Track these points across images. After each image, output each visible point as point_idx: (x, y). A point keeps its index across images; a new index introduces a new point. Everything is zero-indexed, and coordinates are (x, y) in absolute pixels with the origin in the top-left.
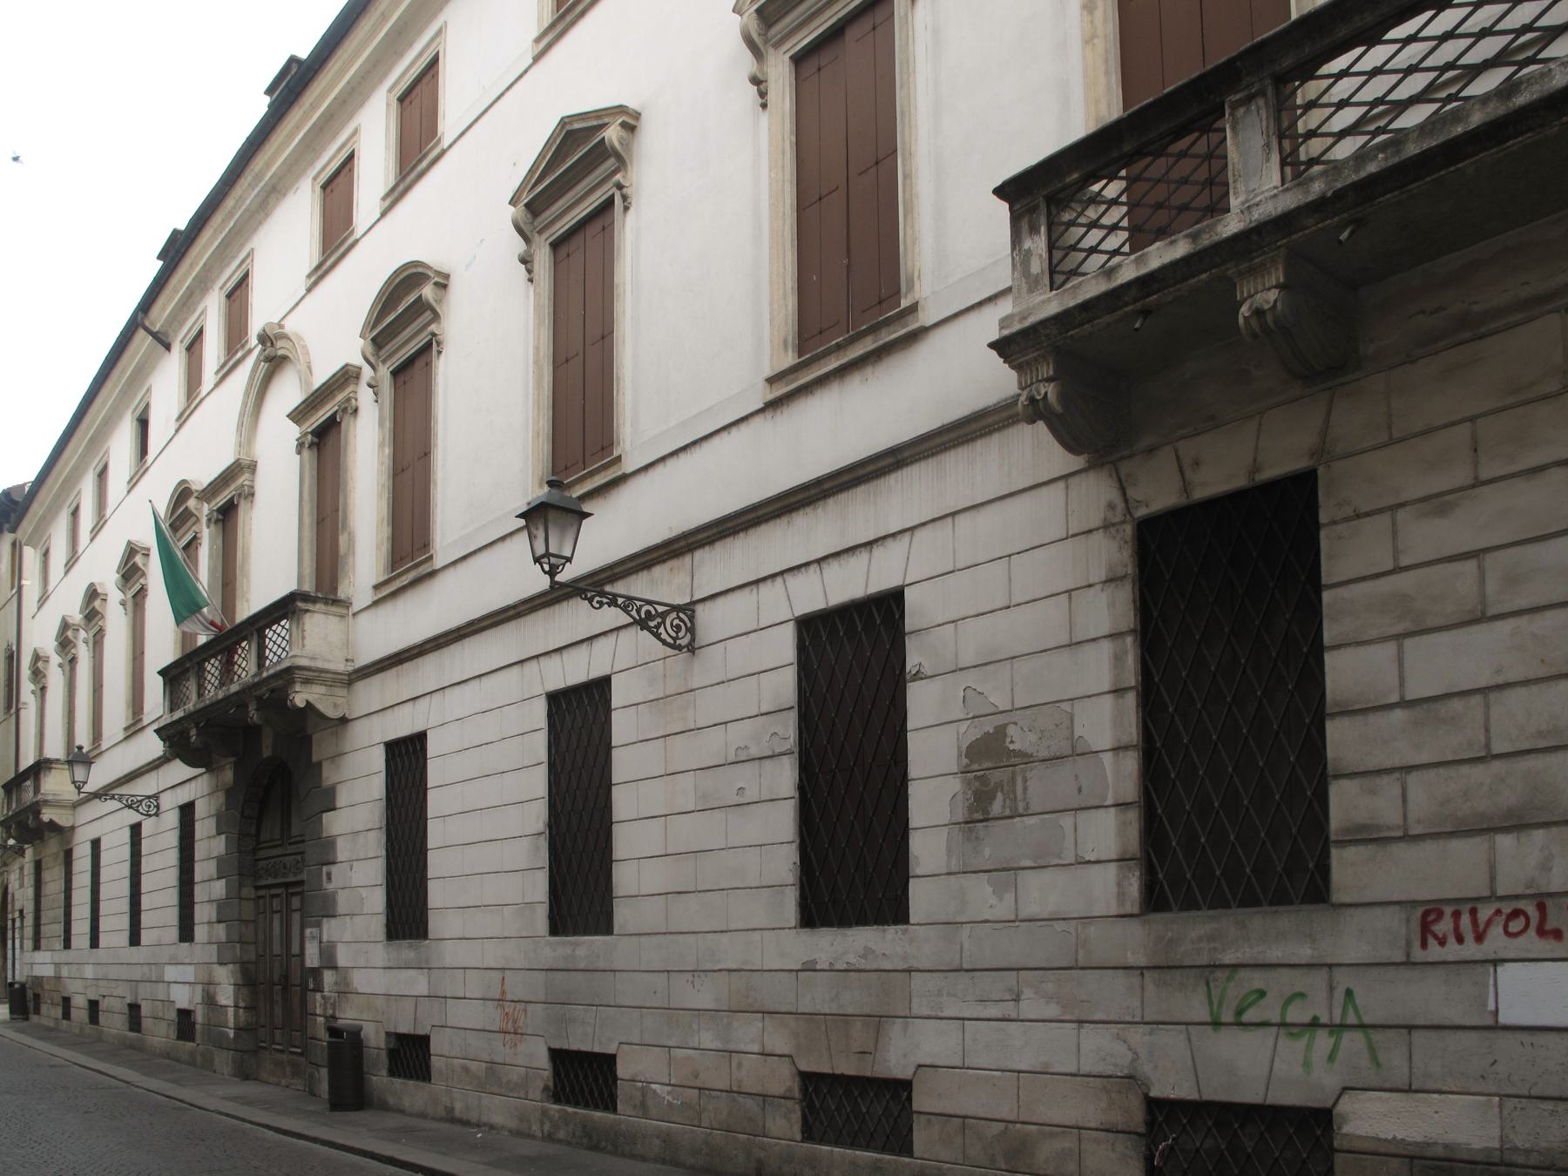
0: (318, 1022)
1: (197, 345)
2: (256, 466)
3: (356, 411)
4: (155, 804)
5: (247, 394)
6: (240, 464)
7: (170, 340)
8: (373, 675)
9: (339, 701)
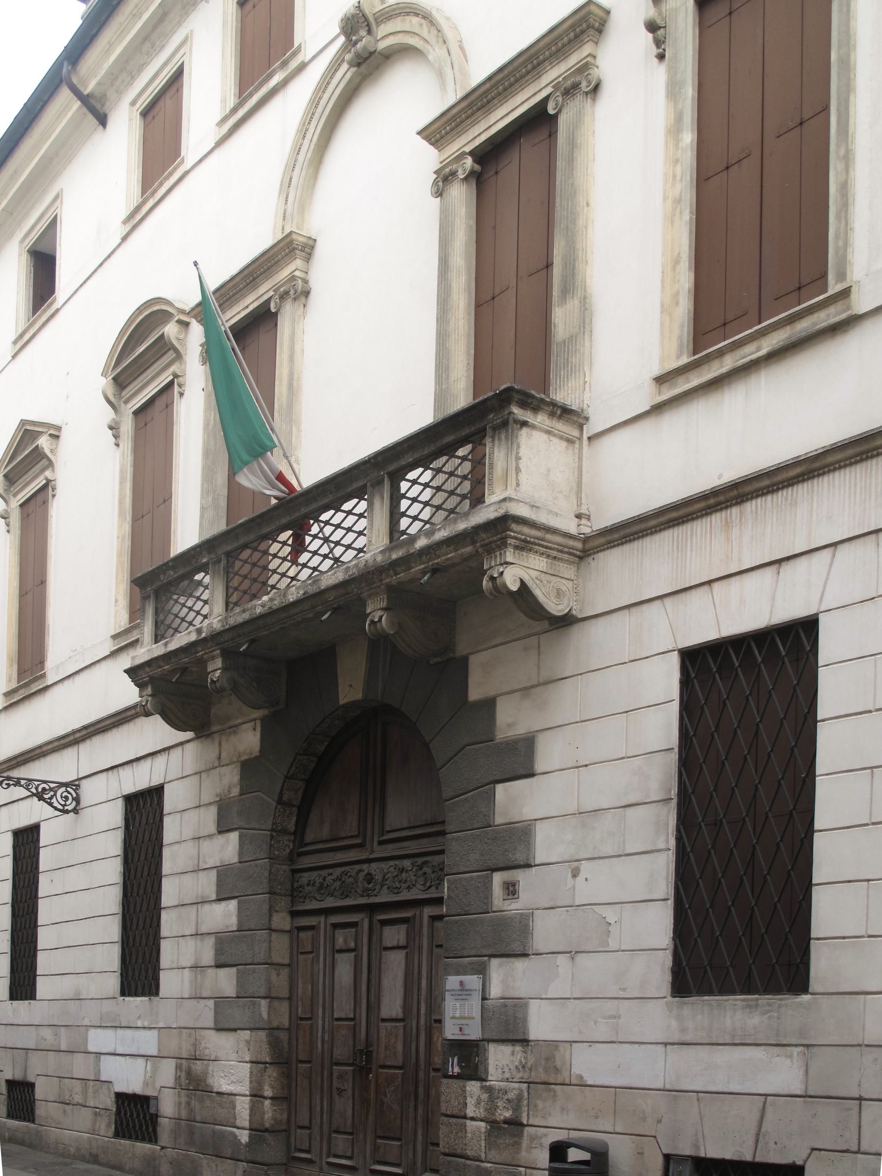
0: (469, 1129)
1: (167, 102)
2: (313, 247)
3: (596, 89)
4: (75, 795)
5: (303, 132)
6: (292, 241)
7: (106, 109)
8: (652, 534)
9: (565, 586)
